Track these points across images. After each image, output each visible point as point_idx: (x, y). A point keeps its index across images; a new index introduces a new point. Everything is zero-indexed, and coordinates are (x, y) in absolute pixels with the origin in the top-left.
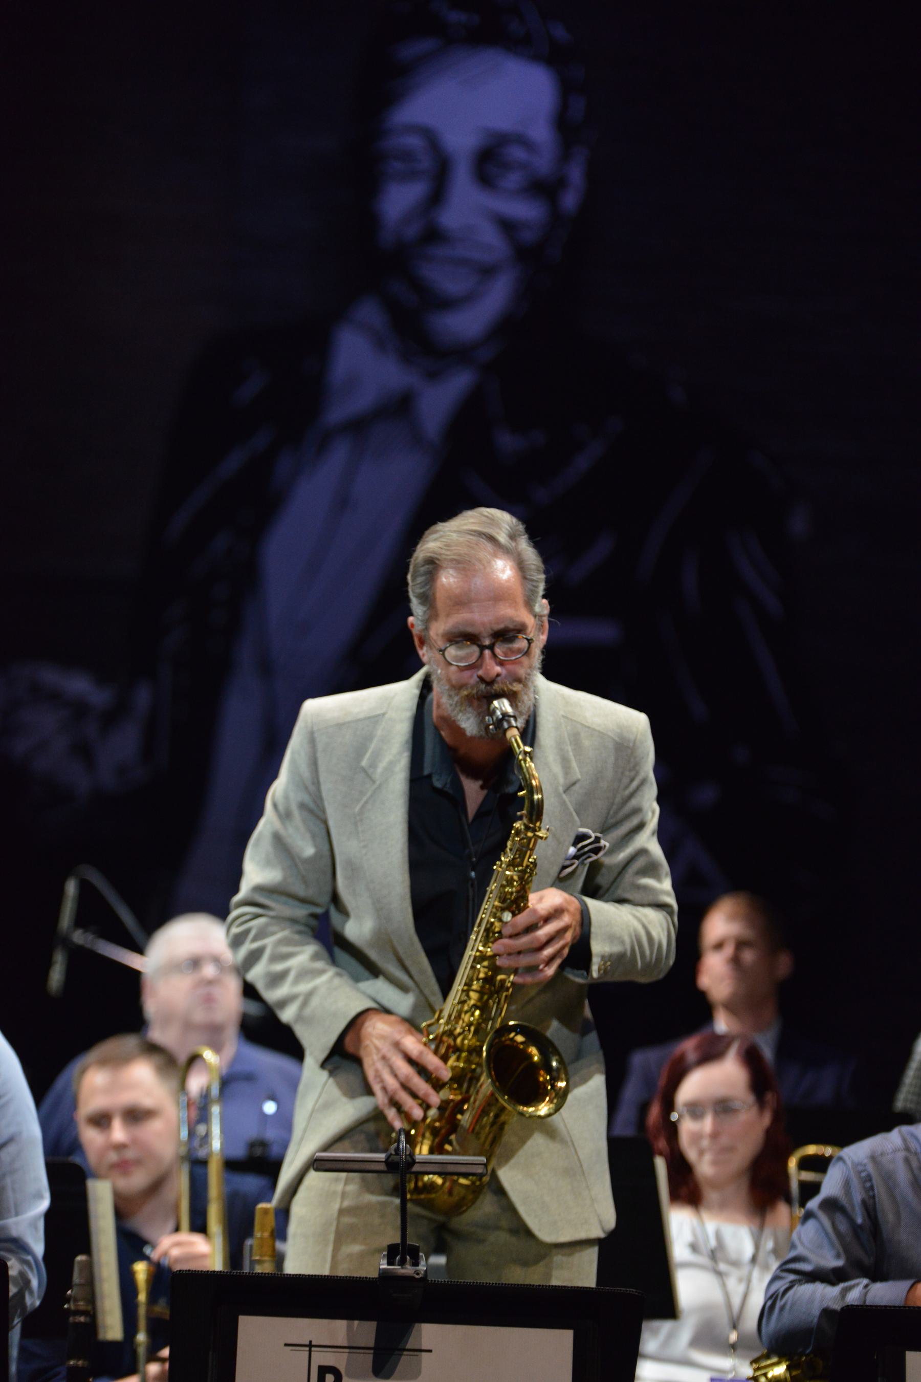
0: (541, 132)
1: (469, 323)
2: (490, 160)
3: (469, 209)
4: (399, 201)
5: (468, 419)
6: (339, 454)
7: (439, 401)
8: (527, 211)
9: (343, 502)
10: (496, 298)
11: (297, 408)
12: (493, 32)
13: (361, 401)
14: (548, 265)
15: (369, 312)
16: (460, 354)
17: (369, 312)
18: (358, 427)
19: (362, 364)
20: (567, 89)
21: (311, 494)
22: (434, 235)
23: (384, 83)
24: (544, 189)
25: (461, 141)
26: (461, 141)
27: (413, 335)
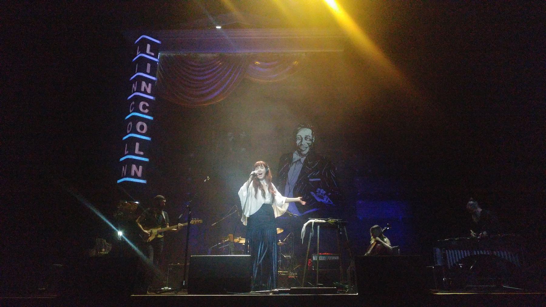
0: (311, 135)
1: (305, 152)
2: (306, 138)
3: (305, 142)
4: (298, 142)
5: (306, 161)
6: (294, 164)
7: (303, 159)
8: (310, 142)
9: (295, 169)
10: (308, 150)
11: (290, 161)
12: (306, 127)
13: (295, 160)
14: (312, 147)
15: (296, 152)
16: (305, 155)
17: (296, 152)
18: (296, 162)
19: (296, 156)
20: (313, 131)
21: (292, 168)
22: (301, 145)
23: (296, 132)
24: (311, 140)
25: (303, 136)
26: (303, 136)
27: (300, 153)
